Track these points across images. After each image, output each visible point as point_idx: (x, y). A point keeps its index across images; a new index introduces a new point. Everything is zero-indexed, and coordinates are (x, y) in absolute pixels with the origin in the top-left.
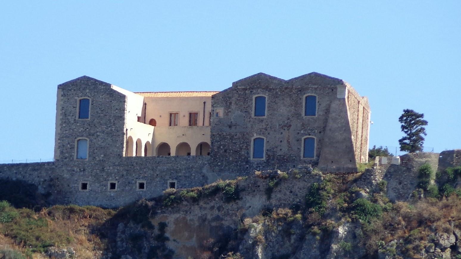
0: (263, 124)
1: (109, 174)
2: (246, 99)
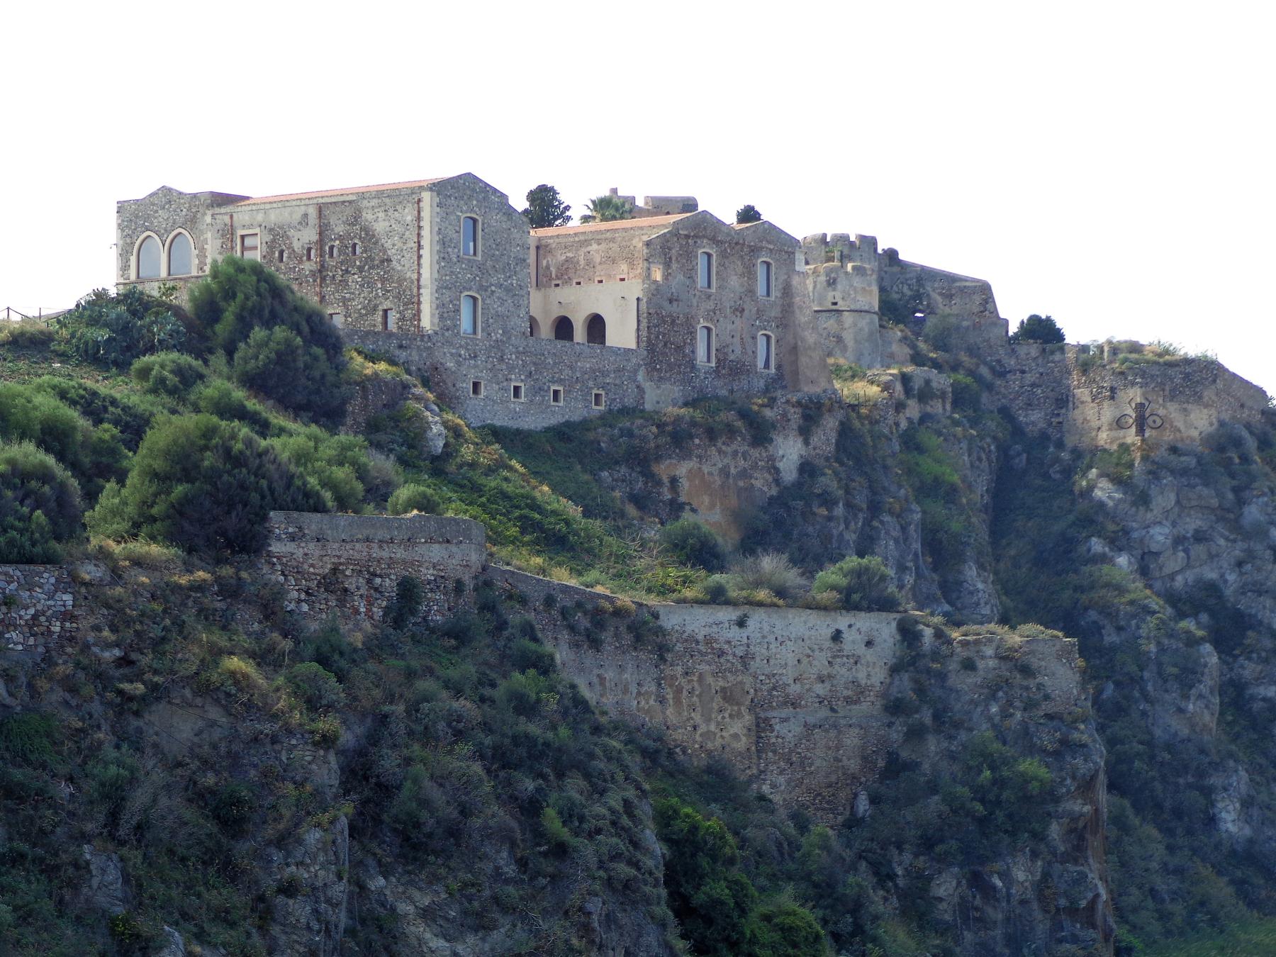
0: (711, 303)
1: (511, 369)
2: (689, 256)
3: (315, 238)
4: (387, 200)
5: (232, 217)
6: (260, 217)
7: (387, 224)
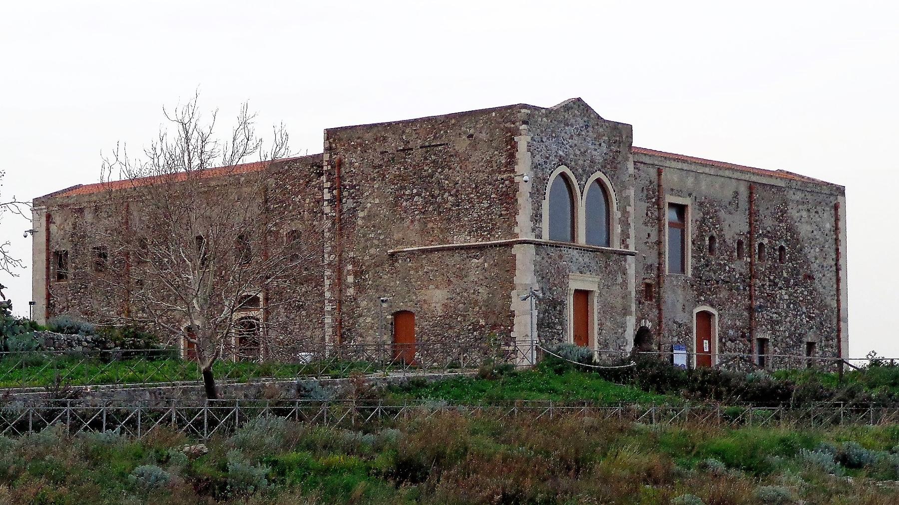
3: (746, 228)
4: (809, 196)
5: (659, 173)
6: (690, 181)
7: (809, 228)
